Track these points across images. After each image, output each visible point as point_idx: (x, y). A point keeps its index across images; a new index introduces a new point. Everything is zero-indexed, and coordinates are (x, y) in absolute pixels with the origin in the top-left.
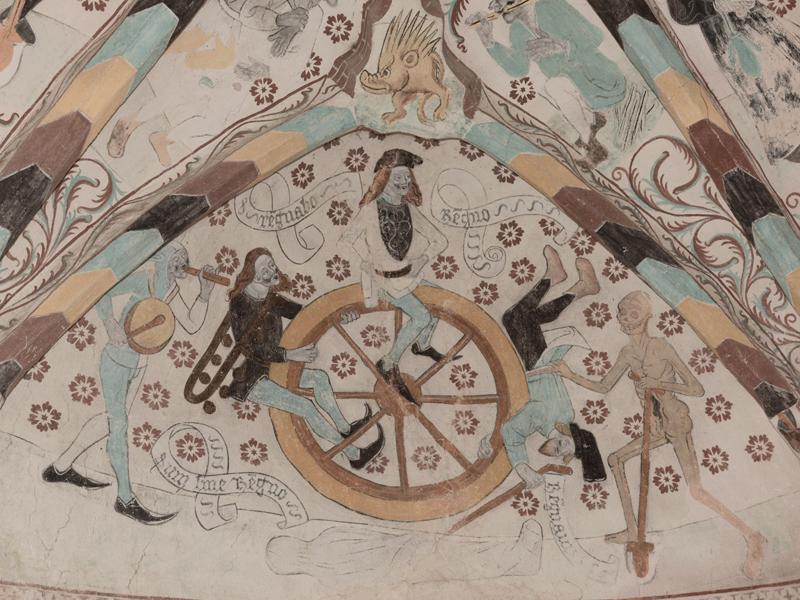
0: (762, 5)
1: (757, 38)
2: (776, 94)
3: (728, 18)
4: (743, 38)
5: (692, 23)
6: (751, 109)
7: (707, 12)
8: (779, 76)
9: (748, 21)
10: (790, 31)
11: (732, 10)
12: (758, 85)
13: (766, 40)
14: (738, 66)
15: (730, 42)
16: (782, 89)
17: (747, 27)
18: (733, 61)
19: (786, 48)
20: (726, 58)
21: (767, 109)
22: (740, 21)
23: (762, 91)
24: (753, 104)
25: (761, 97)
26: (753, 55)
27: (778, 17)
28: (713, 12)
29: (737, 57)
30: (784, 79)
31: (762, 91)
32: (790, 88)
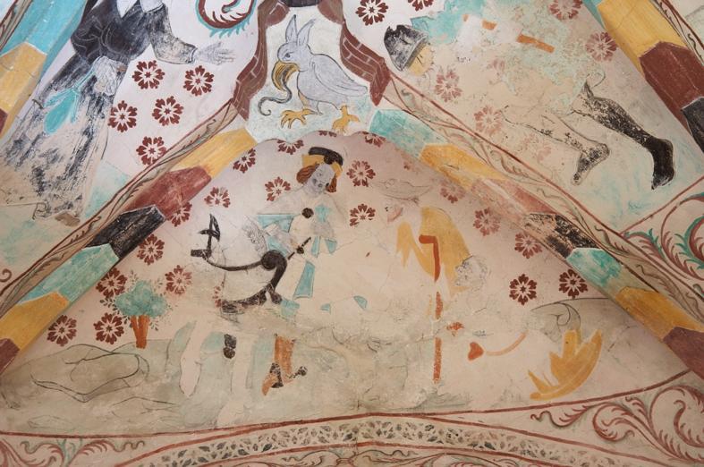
0: (112, 102)
1: (79, 114)
2: (37, 158)
3: (90, 77)
4: (76, 100)
5: (75, 47)
6: (12, 143)
7: (89, 55)
8: (55, 150)
9: (93, 97)
10: (99, 140)
11: (98, 77)
12: (38, 137)
13: (82, 122)
14: (48, 109)
15: (68, 90)
16: (43, 161)
17: (88, 98)
18: (52, 103)
19: (83, 144)
20: (53, 94)
21: (18, 160)
22: (91, 89)
23: (33, 144)
24: (19, 142)
25: (28, 145)
26: (64, 119)
27: (107, 121)
28: (91, 61)
29: (57, 104)
30: (54, 157)
31: (33, 144)
32: (47, 168)
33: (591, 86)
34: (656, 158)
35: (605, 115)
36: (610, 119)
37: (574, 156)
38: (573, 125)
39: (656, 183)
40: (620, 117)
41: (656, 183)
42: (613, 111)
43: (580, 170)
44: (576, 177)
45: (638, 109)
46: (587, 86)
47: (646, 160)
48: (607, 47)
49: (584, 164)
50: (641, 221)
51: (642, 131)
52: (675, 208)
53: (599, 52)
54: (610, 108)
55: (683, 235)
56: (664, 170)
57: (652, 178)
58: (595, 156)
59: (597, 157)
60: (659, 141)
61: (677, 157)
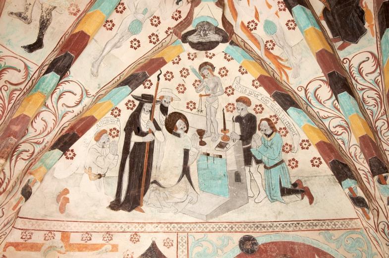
33: (56, 9)
34: (35, 44)
35: (45, 18)
36: (44, 20)
37: (22, 10)
38: (36, 5)
39: (25, 47)
40: (46, 24)
41: (25, 47)
42: (48, 21)
43: (16, 14)
44: (12, 13)
45: (52, 30)
46: (55, 7)
47: (33, 40)
48: (74, 12)
49: (19, 15)
50: (4, 47)
51: (43, 35)
52: (17, 58)
53: (71, 9)
54: (49, 19)
55: (6, 65)
56: (31, 48)
57: (26, 45)
58: (25, 19)
59: (25, 19)
60: (42, 43)
61: (38, 51)
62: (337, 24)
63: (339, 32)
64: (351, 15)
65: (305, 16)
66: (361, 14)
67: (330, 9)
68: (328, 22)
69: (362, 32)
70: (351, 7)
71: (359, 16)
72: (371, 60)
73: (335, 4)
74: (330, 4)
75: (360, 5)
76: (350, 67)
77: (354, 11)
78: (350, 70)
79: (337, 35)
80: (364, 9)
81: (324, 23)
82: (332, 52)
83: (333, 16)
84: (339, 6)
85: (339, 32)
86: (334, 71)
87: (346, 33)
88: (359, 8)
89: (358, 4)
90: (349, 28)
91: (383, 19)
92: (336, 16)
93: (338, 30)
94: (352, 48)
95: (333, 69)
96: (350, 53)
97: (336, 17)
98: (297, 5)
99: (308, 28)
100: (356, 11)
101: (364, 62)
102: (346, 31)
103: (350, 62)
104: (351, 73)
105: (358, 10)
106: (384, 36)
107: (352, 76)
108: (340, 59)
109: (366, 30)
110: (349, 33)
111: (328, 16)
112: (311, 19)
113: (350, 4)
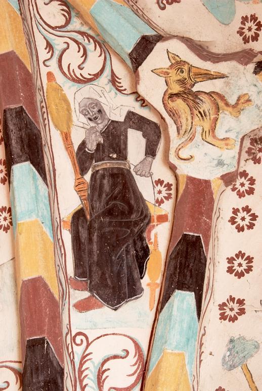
62: (91, 253)
63: (90, 271)
64: (124, 248)
65: (33, 192)
66: (143, 254)
67: (88, 217)
68: (76, 239)
69: (134, 291)
70: (129, 231)
71: (137, 256)
72: (132, 359)
73: (101, 211)
74: (93, 208)
75: (145, 235)
76: (84, 357)
77: (131, 241)
78: (81, 365)
79: (82, 275)
80: (149, 246)
81: (67, 237)
82: (56, 296)
83: (90, 234)
84: (107, 220)
85: (90, 271)
86: (43, 340)
87: (103, 277)
88: (142, 239)
89: (142, 232)
90: (112, 272)
91: (176, 268)
92: (96, 234)
93: (90, 267)
94: (103, 314)
95: (42, 332)
96: (95, 326)
97: (95, 238)
98: (25, 161)
99: (28, 220)
100: (135, 243)
101: (115, 357)
102: (103, 274)
103: (88, 345)
104: (81, 372)
105: (139, 244)
106: (167, 305)
107: (81, 381)
108: (70, 330)
109: (142, 290)
110: (109, 283)
111: (80, 228)
112: (41, 205)
113: (128, 225)
